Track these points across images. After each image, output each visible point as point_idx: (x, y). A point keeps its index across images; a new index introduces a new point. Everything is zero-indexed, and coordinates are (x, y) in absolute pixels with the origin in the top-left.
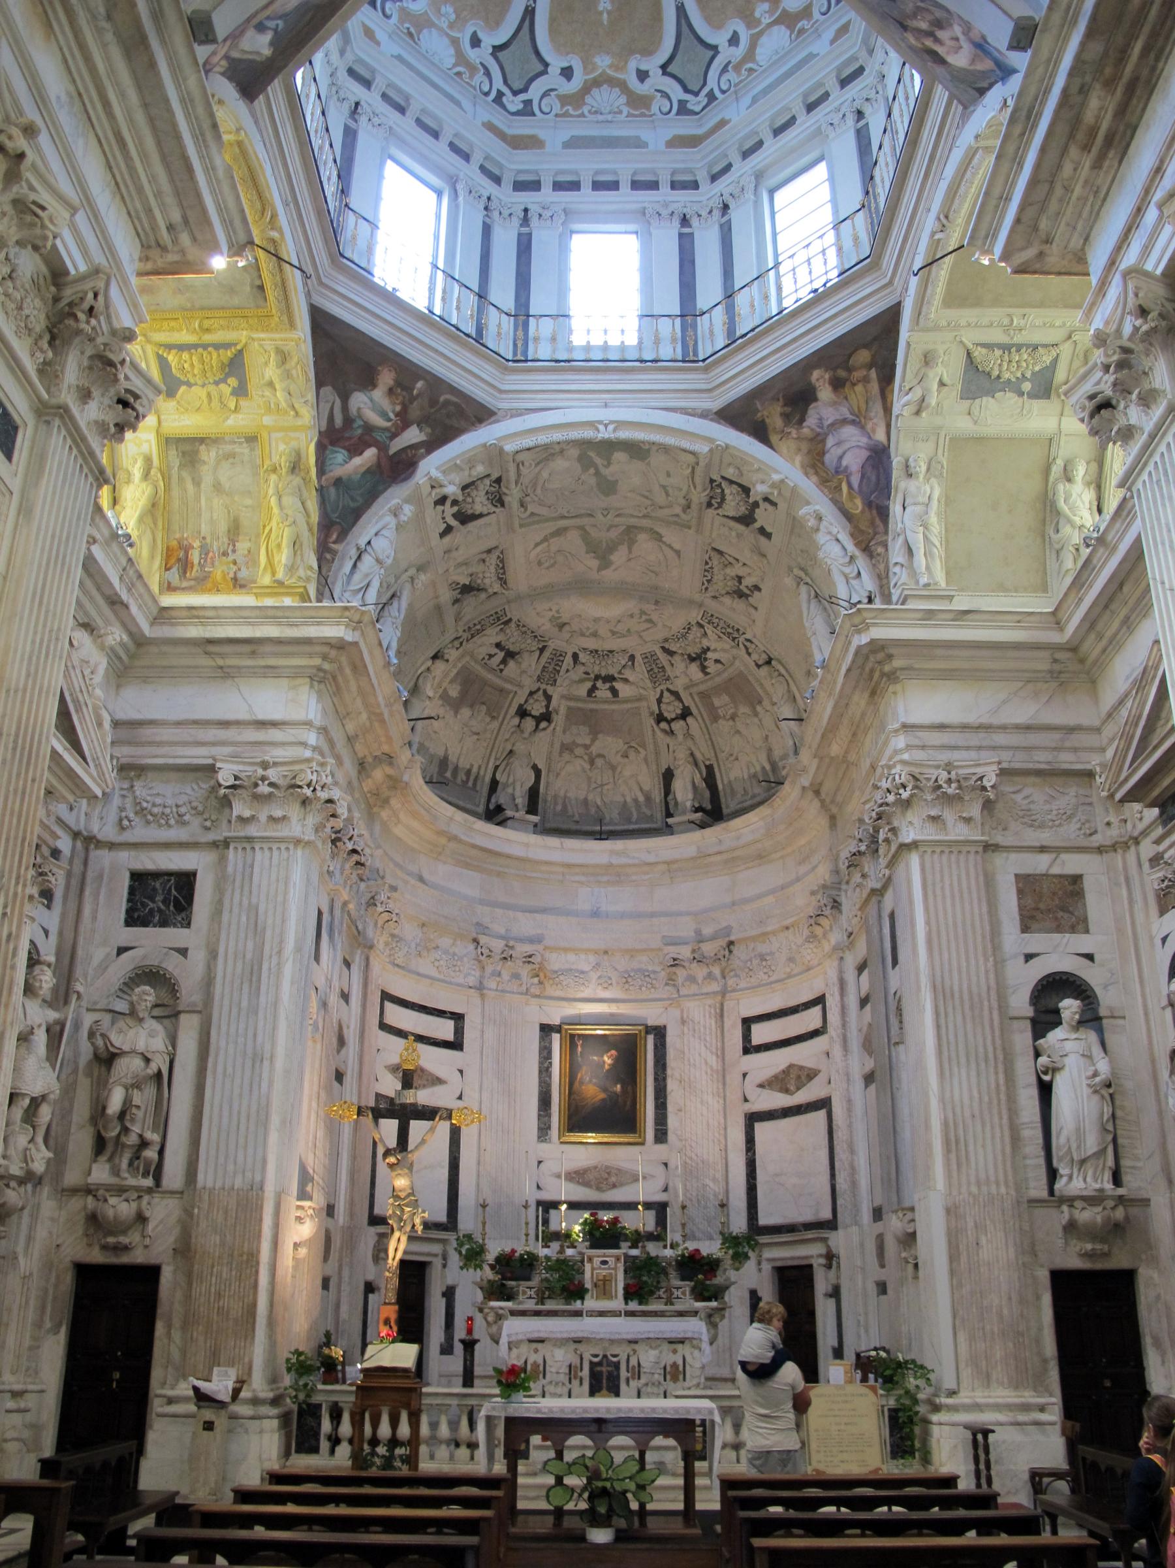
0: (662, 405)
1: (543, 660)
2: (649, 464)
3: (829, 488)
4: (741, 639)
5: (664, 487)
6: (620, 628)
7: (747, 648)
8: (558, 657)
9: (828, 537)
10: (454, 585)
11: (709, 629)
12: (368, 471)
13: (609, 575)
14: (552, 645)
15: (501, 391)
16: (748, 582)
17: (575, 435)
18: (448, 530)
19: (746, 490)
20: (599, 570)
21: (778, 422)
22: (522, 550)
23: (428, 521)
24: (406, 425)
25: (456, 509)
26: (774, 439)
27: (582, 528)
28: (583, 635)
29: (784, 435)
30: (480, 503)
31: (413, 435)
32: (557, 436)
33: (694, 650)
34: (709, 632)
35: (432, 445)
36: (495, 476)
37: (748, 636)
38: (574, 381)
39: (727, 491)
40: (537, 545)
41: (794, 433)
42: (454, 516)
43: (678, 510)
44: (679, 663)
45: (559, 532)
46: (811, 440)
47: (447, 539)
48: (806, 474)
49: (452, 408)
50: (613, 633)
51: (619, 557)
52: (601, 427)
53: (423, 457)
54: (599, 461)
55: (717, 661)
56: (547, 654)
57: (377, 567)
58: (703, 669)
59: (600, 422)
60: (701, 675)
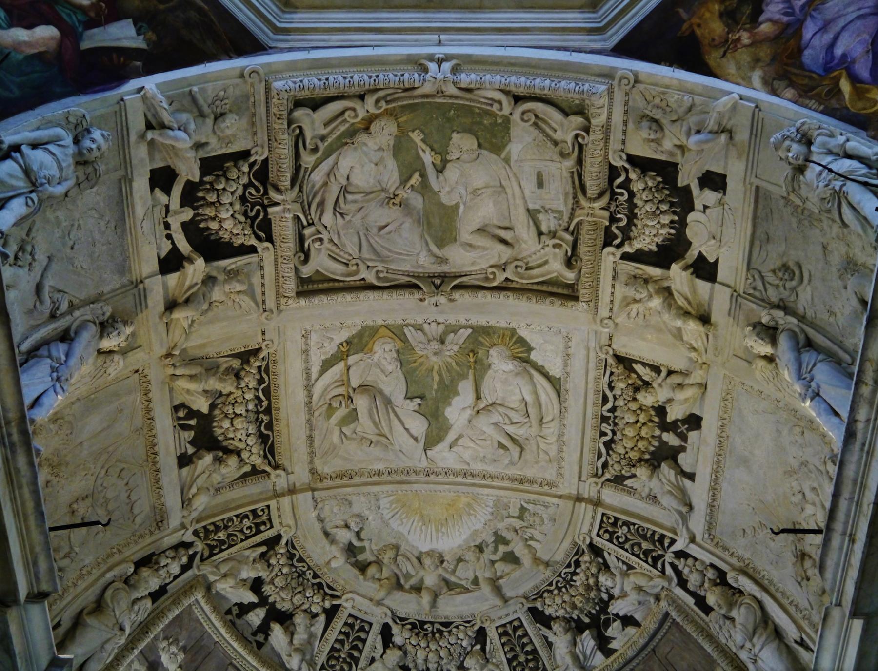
0: (529, 44)
1: (333, 635)
2: (507, 160)
3: (818, 98)
4: (669, 557)
5: (532, 214)
6: (464, 574)
7: (678, 572)
8: (357, 628)
9: (829, 158)
10: (183, 413)
11: (612, 552)
12: (39, 57)
13: (443, 456)
14: (349, 605)
15: (277, 30)
16: (674, 413)
17: (389, 77)
18: (171, 263)
19: (666, 171)
20: (431, 441)
21: (717, 28)
22: (303, 338)
23: (140, 211)
24: (115, 15)
25: (188, 214)
26: (713, 58)
27: (397, 332)
28: (399, 586)
29: (728, 46)
30: (228, 224)
31: (123, 34)
32: (361, 78)
33: (583, 609)
34: (611, 561)
35: (155, 61)
36: (259, 157)
37: (677, 547)
38: (389, 20)
39: (637, 186)
40: (327, 365)
41: (745, 38)
42: (185, 226)
43: (556, 267)
44: (561, 640)
45: (359, 343)
46: (774, 39)
47: (172, 279)
48: (774, 92)
49: (192, 14)
50: (450, 586)
51: (457, 412)
52: (433, 66)
53: (139, 75)
54: (428, 157)
55: (628, 621)
56: (338, 624)
57: (21, 184)
58: (603, 645)
59: (431, 58)
60: (599, 656)
